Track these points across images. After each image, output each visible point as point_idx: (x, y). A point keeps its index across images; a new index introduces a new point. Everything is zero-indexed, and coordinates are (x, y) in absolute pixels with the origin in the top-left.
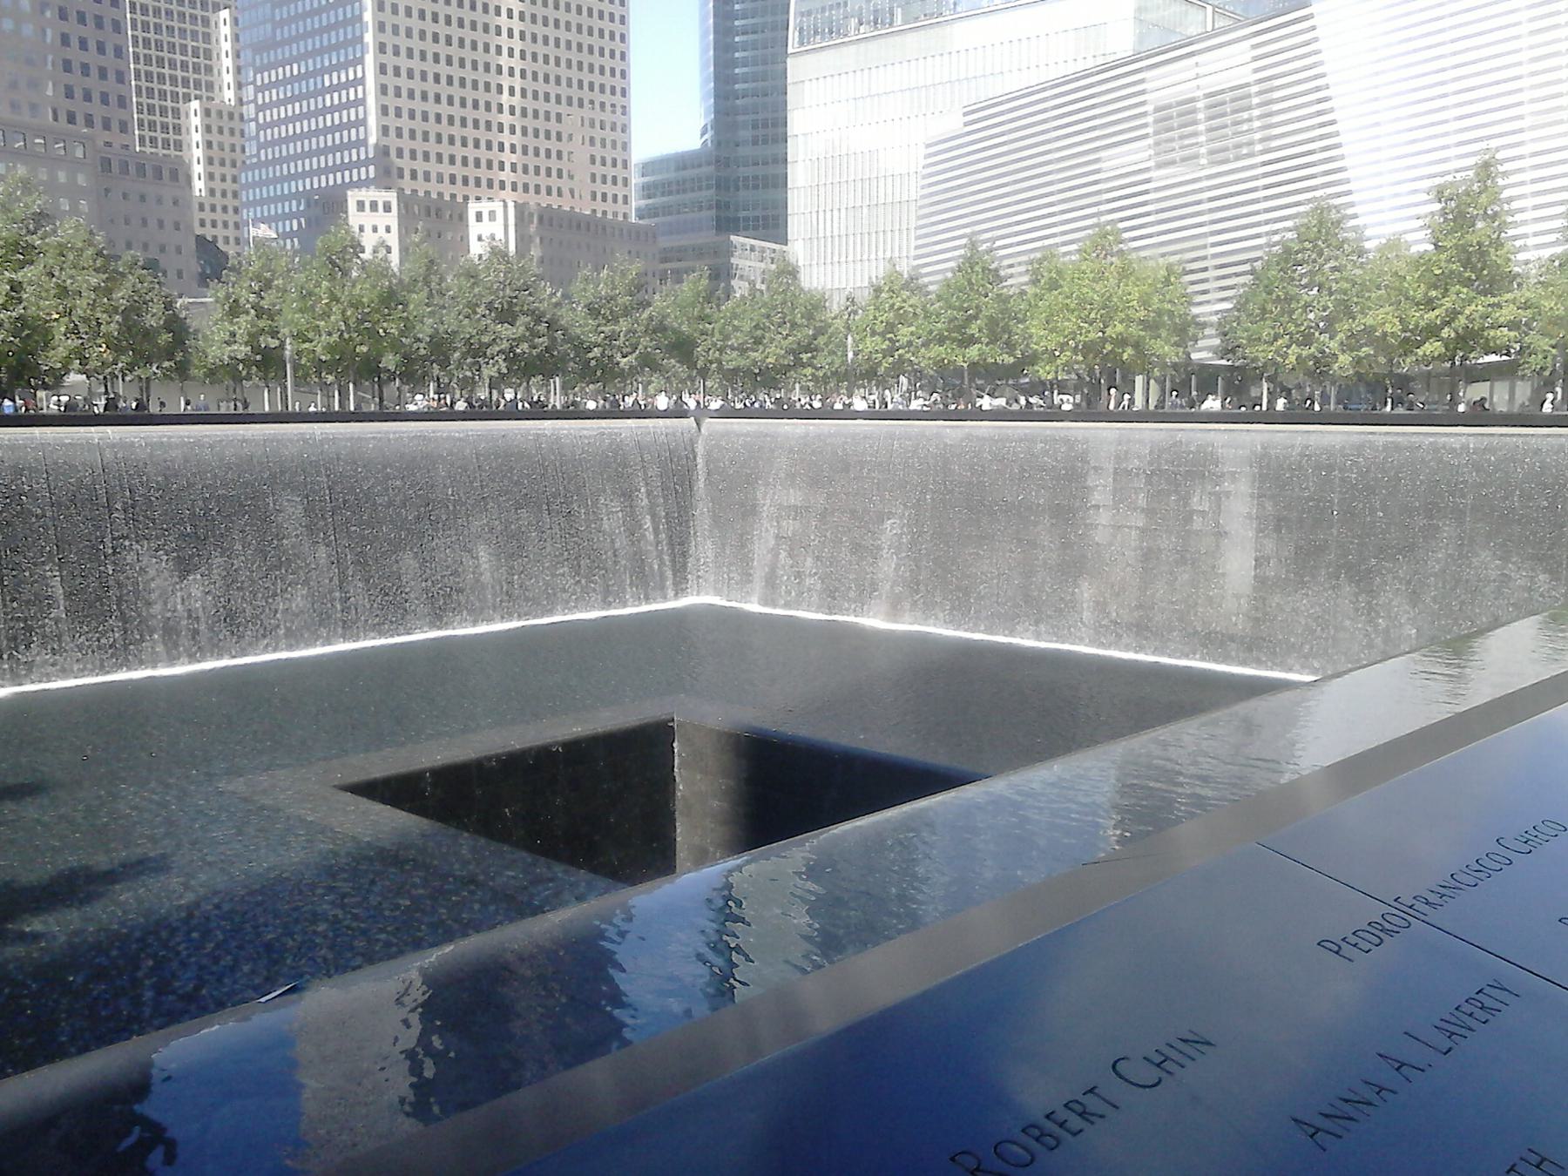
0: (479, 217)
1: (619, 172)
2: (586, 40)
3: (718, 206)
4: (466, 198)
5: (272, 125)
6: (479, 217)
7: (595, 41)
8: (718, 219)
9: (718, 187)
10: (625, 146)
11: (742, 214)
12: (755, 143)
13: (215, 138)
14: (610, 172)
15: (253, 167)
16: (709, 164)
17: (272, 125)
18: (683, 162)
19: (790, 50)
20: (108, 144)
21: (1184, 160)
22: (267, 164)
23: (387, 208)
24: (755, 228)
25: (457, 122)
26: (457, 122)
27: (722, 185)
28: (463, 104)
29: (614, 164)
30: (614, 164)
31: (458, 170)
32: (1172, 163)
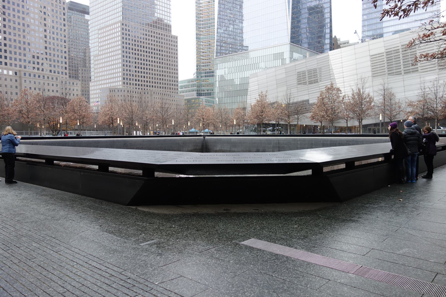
1: (176, 83)
2: (168, 54)
3: (197, 91)
4: (142, 89)
5: (98, 73)
7: (171, 55)
8: (197, 93)
10: (177, 78)
12: (205, 77)
14: (174, 83)
15: (93, 82)
16: (195, 81)
17: (98, 73)
18: (189, 81)
19: (215, 57)
21: (303, 83)
22: (96, 81)
24: (206, 95)
25: (140, 72)
26: (140, 72)
28: (141, 68)
29: (175, 81)
30: (175, 81)
31: (140, 83)
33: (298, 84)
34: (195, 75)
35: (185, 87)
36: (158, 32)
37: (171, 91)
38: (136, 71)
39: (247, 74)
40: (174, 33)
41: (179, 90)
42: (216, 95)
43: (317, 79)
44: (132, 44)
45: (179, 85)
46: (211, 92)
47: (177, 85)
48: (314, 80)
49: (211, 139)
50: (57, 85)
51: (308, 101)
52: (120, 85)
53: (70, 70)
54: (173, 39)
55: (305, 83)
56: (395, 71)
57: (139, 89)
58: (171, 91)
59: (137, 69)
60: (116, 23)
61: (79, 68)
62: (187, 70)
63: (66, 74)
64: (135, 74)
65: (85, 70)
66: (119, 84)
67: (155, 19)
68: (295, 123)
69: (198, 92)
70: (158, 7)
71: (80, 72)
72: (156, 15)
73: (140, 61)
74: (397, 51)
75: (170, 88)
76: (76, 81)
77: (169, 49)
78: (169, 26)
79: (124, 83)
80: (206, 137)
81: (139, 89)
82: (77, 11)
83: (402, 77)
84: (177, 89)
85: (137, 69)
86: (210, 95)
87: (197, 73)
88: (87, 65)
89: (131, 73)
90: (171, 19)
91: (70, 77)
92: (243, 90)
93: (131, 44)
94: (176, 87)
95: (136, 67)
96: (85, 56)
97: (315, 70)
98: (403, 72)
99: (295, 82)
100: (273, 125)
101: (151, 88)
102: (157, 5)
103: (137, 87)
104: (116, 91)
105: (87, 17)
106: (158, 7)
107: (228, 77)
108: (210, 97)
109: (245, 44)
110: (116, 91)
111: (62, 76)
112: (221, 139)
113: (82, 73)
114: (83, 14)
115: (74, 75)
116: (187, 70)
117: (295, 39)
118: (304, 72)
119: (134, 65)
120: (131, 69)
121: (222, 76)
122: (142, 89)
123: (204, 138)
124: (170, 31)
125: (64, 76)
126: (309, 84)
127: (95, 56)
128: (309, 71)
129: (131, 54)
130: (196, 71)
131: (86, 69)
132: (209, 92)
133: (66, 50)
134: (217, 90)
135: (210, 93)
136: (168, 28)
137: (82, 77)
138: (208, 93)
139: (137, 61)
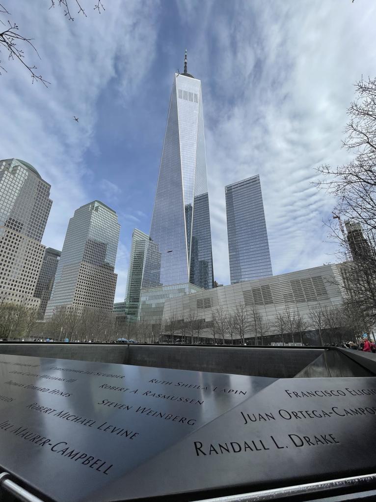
1: (111, 305)
10: (113, 301)
35: (118, 308)
37: (108, 310)
39: (161, 301)
41: (113, 310)
42: (139, 315)
49: (133, 347)
51: (204, 320)
53: (36, 291)
55: (202, 307)
62: (120, 296)
68: (197, 336)
74: (259, 290)
76: (37, 299)
78: (113, 268)
82: (52, 253)
83: (263, 306)
91: (34, 296)
92: (159, 311)
100: (180, 337)
105: (58, 258)
107: (147, 303)
109: (162, 281)
112: (141, 347)
115: (37, 295)
116: (120, 296)
117: (192, 281)
121: (144, 302)
126: (205, 308)
127: (57, 283)
128: (205, 299)
134: (140, 310)
136: (112, 269)
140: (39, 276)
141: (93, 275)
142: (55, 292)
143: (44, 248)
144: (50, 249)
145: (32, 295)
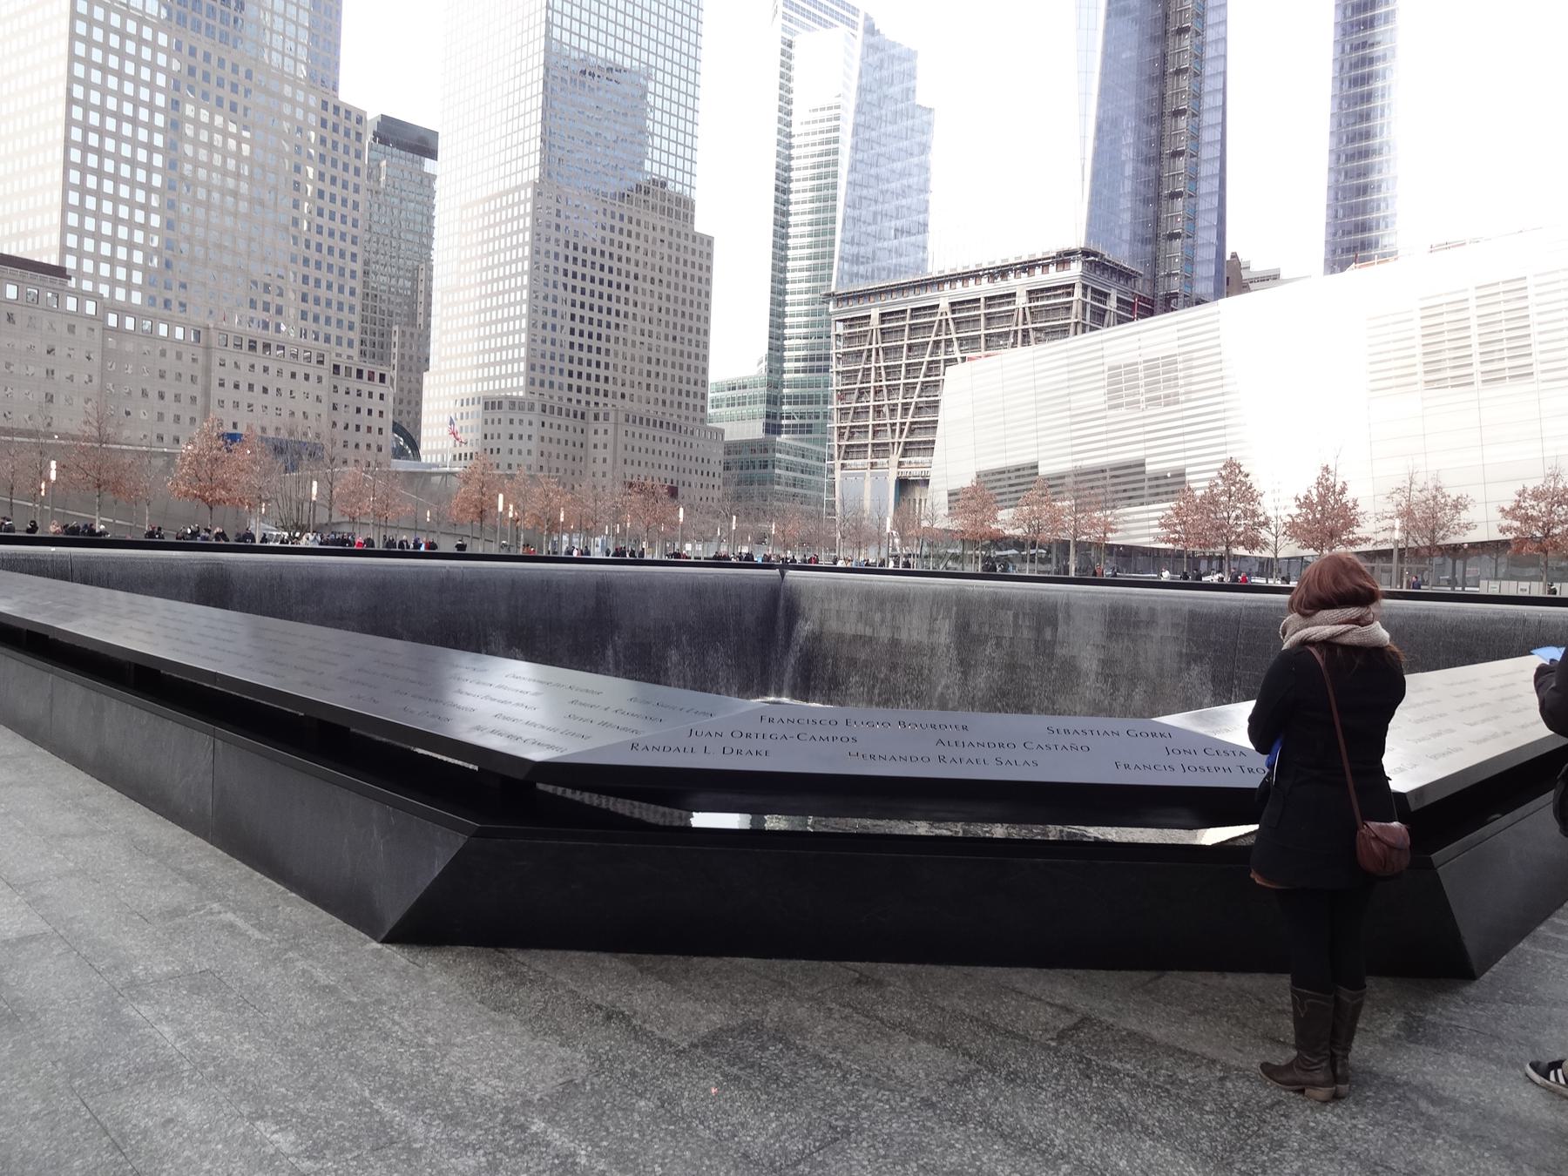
0: (596, 417)
1: (699, 389)
2: (681, 295)
4: (588, 403)
6: (596, 417)
8: (767, 425)
9: (768, 402)
10: (705, 371)
11: (784, 422)
13: (407, 352)
20: (338, 355)
21: (1128, 404)
23: (532, 408)
27: (773, 400)
32: (1120, 406)
33: (1111, 408)
34: (765, 363)
36: (651, 221)
37: (683, 412)
38: (572, 345)
40: (701, 226)
43: (1177, 394)
44: (567, 258)
45: (710, 395)
46: (813, 421)
47: (704, 396)
48: (1167, 396)
50: (320, 379)
52: (518, 388)
54: (697, 247)
56: (1449, 373)
57: (579, 402)
58: (683, 412)
59: (576, 339)
60: (518, 188)
61: (396, 328)
63: (350, 344)
64: (568, 352)
65: (412, 335)
66: (516, 386)
67: (642, 179)
69: (771, 421)
70: (657, 140)
71: (396, 339)
72: (647, 164)
73: (587, 313)
75: (680, 404)
77: (685, 276)
79: (532, 382)
80: (790, 573)
81: (579, 402)
82: (400, 145)
84: (703, 409)
85: (576, 339)
86: (809, 432)
87: (770, 358)
88: (420, 320)
89: (558, 350)
90: (697, 182)
91: (363, 353)
93: (562, 258)
94: (699, 402)
95: (572, 332)
96: (415, 291)
97: (1170, 361)
98: (1478, 378)
99: (1098, 398)
101: (619, 402)
102: (652, 134)
103: (574, 395)
104: (506, 405)
105: (429, 165)
106: (657, 140)
108: (808, 440)
110: (506, 405)
111: (339, 350)
113: (403, 346)
114: (417, 157)
118: (1131, 367)
119: (568, 324)
120: (557, 335)
122: (588, 403)
123: (783, 575)
124: (689, 218)
125: (345, 350)
128: (1151, 365)
129: (561, 288)
130: (766, 351)
131: (416, 331)
132: (807, 421)
133: (358, 267)
135: (810, 426)
136: (682, 208)
137: (403, 356)
138: (802, 426)
139: (578, 311)
140: (366, 263)
141: (599, 246)
142: (446, 332)
143: (359, 120)
144: (386, 121)
145: (355, 352)
